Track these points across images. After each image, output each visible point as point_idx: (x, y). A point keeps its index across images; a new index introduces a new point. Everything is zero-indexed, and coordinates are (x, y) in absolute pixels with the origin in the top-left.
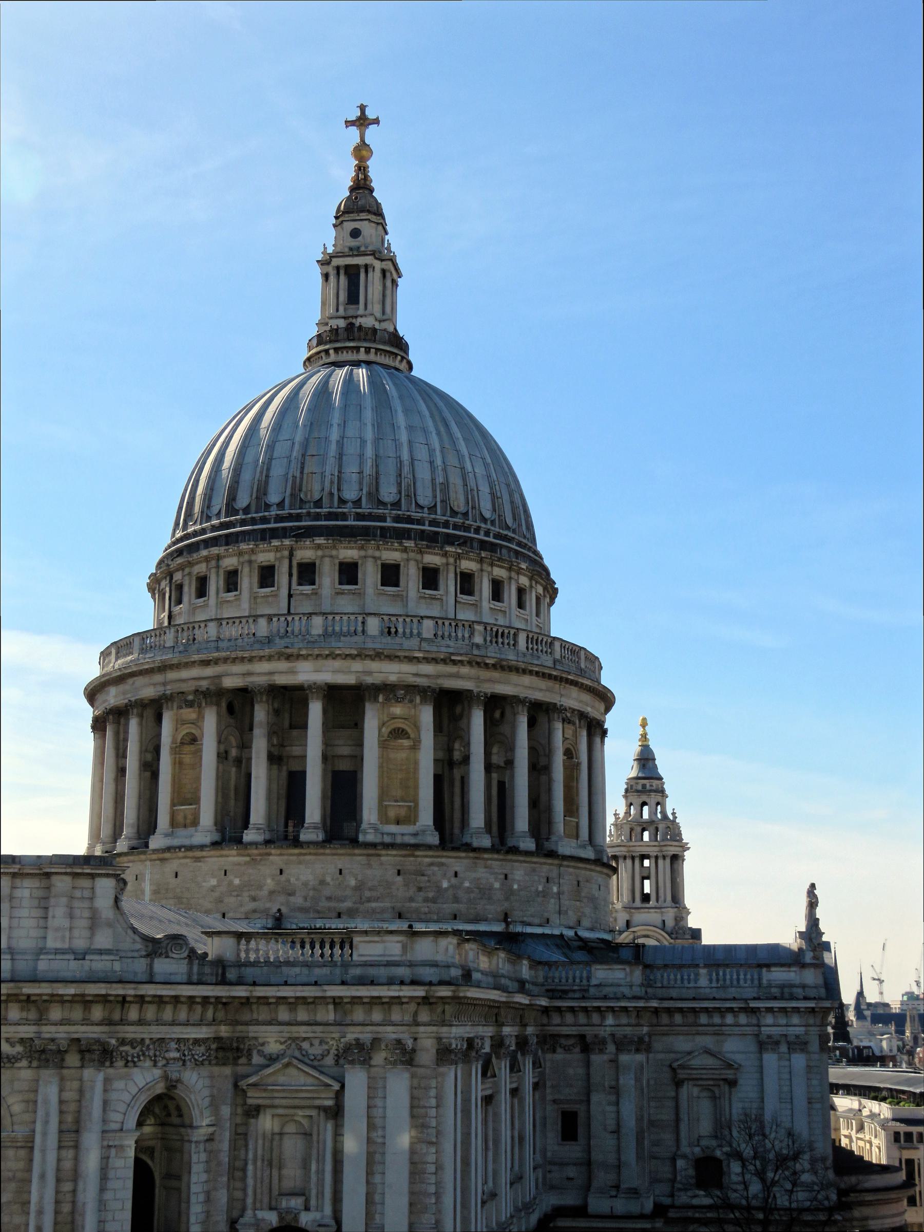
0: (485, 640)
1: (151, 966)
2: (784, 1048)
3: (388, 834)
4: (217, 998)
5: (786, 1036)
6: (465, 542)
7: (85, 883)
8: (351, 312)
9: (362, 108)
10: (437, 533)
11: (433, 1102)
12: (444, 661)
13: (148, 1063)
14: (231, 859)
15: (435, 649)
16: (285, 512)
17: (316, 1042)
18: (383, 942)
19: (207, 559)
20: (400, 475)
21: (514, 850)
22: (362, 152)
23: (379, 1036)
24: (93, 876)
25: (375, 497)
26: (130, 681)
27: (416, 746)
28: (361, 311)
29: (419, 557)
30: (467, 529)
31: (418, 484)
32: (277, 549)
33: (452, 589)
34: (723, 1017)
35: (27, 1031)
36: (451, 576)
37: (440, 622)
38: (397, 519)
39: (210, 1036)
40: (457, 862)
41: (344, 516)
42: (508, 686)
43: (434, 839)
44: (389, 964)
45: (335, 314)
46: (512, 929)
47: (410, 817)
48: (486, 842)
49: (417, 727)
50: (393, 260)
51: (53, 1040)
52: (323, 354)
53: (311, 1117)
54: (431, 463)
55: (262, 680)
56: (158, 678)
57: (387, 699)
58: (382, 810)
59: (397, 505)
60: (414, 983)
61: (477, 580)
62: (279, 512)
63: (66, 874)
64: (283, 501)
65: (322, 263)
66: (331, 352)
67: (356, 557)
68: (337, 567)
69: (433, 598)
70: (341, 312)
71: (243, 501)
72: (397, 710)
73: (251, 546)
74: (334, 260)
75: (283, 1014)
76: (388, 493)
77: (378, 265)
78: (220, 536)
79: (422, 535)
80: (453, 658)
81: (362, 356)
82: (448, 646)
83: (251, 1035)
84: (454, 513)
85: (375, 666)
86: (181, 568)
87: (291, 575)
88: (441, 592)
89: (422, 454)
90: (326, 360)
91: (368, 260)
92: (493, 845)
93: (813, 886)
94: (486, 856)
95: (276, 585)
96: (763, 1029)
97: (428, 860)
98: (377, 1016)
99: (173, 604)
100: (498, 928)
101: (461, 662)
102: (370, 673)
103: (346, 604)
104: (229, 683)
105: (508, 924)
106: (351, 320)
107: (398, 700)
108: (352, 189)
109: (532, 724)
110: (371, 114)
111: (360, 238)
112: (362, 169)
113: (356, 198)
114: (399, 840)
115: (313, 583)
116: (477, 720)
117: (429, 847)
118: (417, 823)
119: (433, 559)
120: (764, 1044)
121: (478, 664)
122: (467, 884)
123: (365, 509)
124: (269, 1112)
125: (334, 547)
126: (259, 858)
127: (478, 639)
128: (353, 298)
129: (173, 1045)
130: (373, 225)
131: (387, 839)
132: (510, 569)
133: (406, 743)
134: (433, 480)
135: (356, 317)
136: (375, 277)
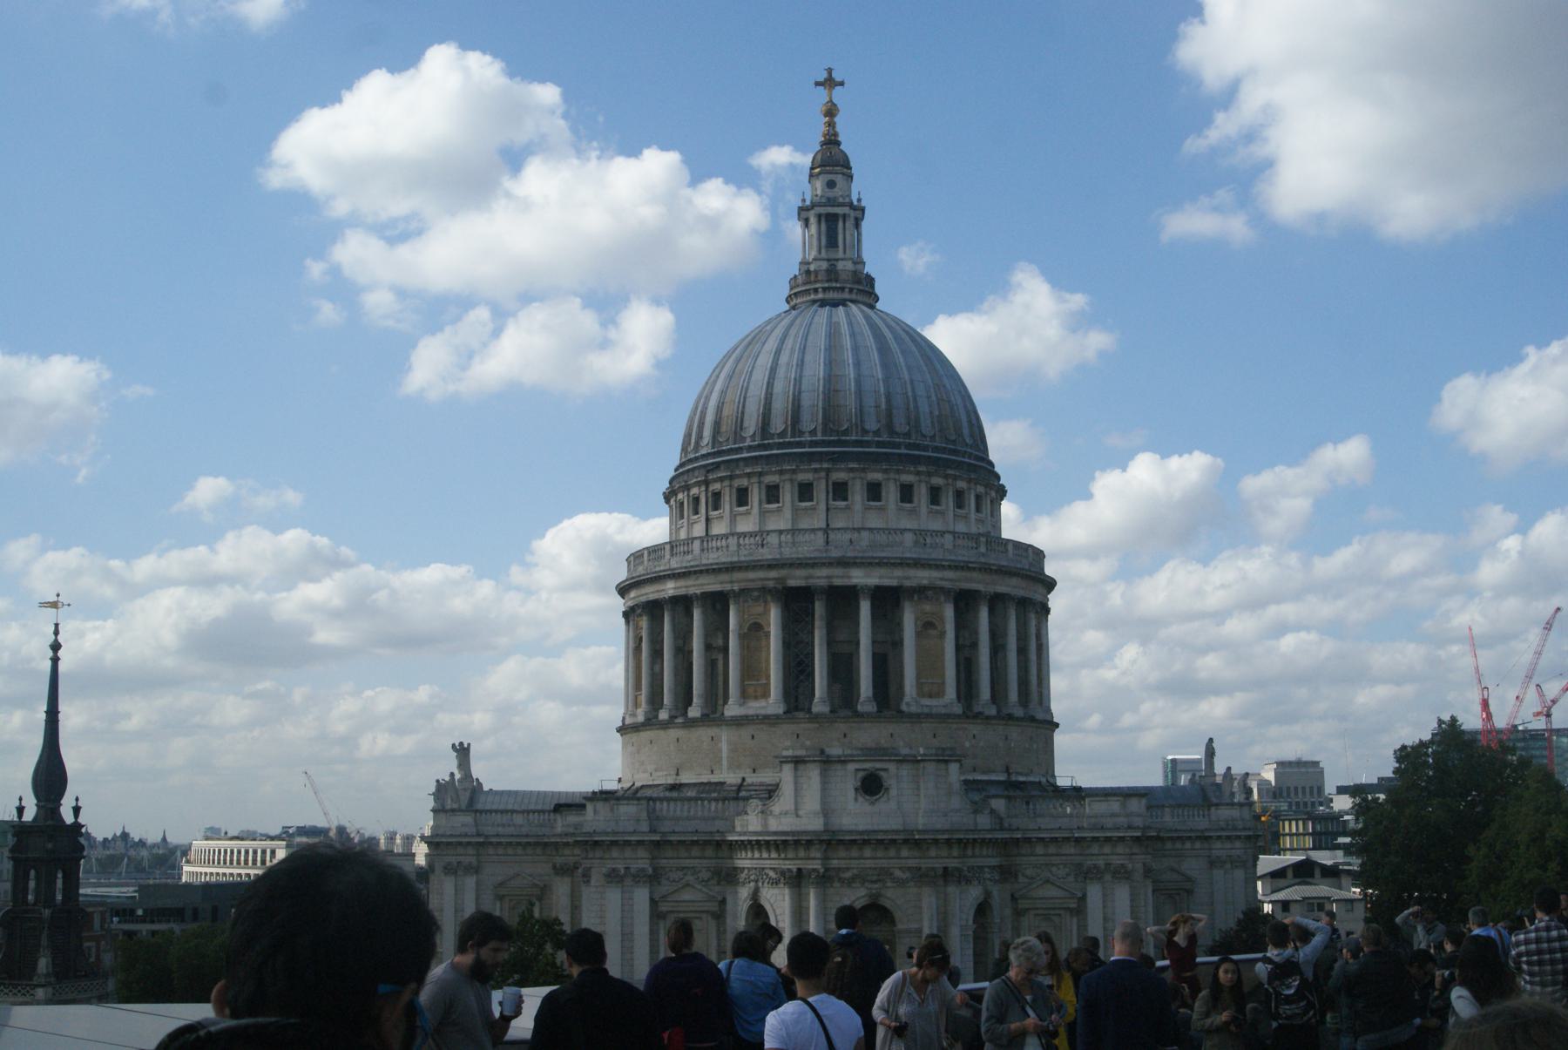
0: (987, 549)
1: (975, 819)
2: (1228, 866)
3: (927, 706)
4: (1002, 839)
5: (1230, 856)
6: (958, 465)
7: (943, 766)
8: (832, 256)
9: (830, 71)
10: (939, 459)
11: (1143, 904)
12: (962, 568)
13: (976, 882)
14: (802, 725)
15: (953, 558)
16: (819, 437)
17: (1061, 867)
18: (1108, 801)
19: (749, 475)
20: (908, 409)
21: (1010, 717)
22: (831, 112)
23: (1109, 862)
24: (946, 762)
25: (890, 427)
26: (694, 577)
27: (942, 634)
28: (840, 254)
29: (927, 479)
30: (955, 452)
31: (922, 417)
32: (816, 470)
33: (951, 504)
34: (1183, 844)
35: (912, 863)
36: (951, 493)
37: (956, 535)
38: (909, 446)
39: (996, 864)
40: (975, 728)
41: (868, 444)
42: (1002, 587)
43: (958, 709)
44: (1113, 815)
45: (819, 257)
46: (1013, 778)
47: (940, 693)
48: (993, 711)
49: (942, 620)
50: (863, 210)
51: (933, 869)
52: (812, 291)
53: (1060, 915)
54: (929, 397)
55: (823, 582)
56: (724, 577)
57: (920, 599)
58: (919, 685)
59: (908, 435)
60: (1130, 827)
61: (966, 495)
62: (814, 438)
63: (934, 760)
64: (816, 427)
65: (801, 209)
66: (820, 290)
67: (881, 479)
68: (865, 488)
69: (937, 512)
70: (824, 255)
71: (778, 425)
72: (928, 607)
73: (794, 467)
74: (815, 208)
75: (1039, 850)
76: (900, 425)
77: (852, 213)
78: (761, 456)
79: (930, 461)
80: (970, 565)
81: (846, 295)
82: (964, 556)
83: (1018, 862)
84: (948, 441)
85: (912, 572)
86: (721, 479)
87: (828, 492)
88: (943, 507)
89: (921, 391)
90: (812, 297)
91: (846, 210)
92: (964, 712)
93: (1211, 740)
94: (993, 722)
95: (815, 500)
96: (1213, 851)
97: (955, 726)
98: (1107, 850)
99: (710, 508)
100: (1002, 777)
101: (974, 569)
102: (908, 578)
103: (874, 521)
104: (792, 583)
105: (1009, 774)
106: (833, 262)
107: (927, 598)
108: (823, 144)
109: (991, 611)
110: (837, 76)
111: (836, 190)
112: (831, 125)
113: (831, 153)
114: (934, 711)
115: (845, 499)
116: (984, 615)
117: (958, 716)
118: (946, 697)
119: (937, 481)
120: (1213, 863)
121: (985, 569)
122: (982, 744)
123: (885, 438)
124: (1032, 912)
125: (863, 470)
126: (827, 724)
127: (983, 549)
128: (832, 242)
129: (986, 870)
130: (845, 177)
131: (926, 710)
132: (986, 486)
133: (933, 632)
134: (931, 413)
135: (837, 260)
136: (850, 224)
